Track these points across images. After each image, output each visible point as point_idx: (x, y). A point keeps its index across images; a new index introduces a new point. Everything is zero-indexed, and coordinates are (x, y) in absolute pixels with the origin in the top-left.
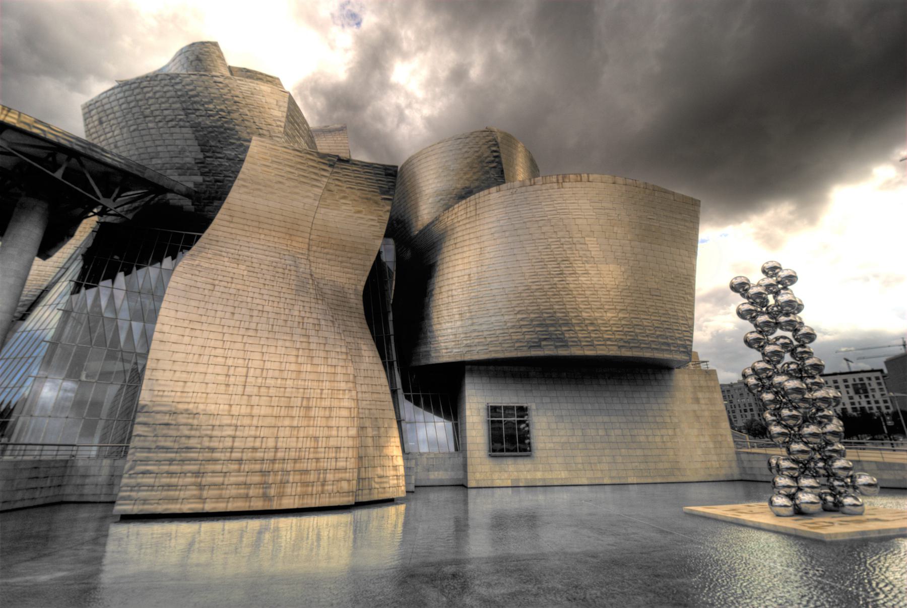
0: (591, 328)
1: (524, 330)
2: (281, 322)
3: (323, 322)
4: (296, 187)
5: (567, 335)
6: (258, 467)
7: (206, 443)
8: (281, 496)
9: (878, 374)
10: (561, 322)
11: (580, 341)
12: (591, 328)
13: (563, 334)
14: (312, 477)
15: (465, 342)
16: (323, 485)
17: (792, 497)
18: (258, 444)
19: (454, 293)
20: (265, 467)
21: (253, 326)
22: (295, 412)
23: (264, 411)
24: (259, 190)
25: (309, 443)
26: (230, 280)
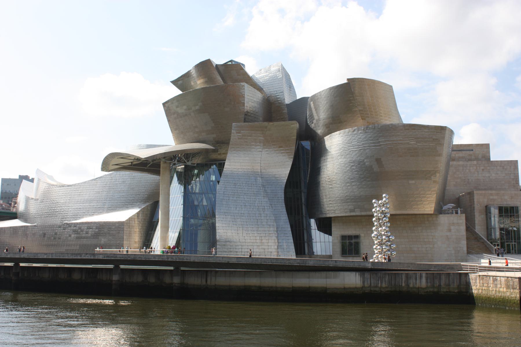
2: (252, 209)
3: (266, 207)
4: (252, 142)
7: (235, 250)
21: (243, 212)
22: (258, 241)
23: (249, 241)
24: (239, 148)
25: (262, 251)
26: (233, 194)
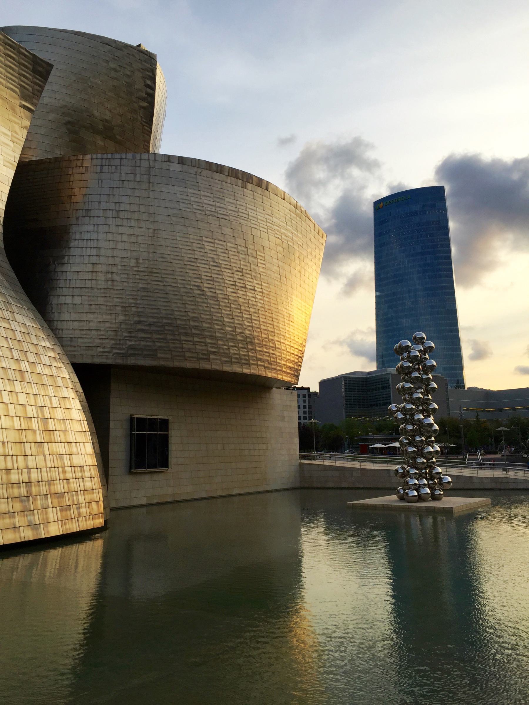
0: (250, 347)
1: (196, 339)
5: (232, 351)
6: (16, 492)
8: (47, 523)
9: (306, 392)
10: (229, 336)
11: (241, 359)
12: (250, 347)
13: (229, 349)
14: (67, 501)
15: (129, 343)
16: (78, 508)
17: (417, 490)
18: (9, 465)
19: (116, 277)
20: (23, 491)
